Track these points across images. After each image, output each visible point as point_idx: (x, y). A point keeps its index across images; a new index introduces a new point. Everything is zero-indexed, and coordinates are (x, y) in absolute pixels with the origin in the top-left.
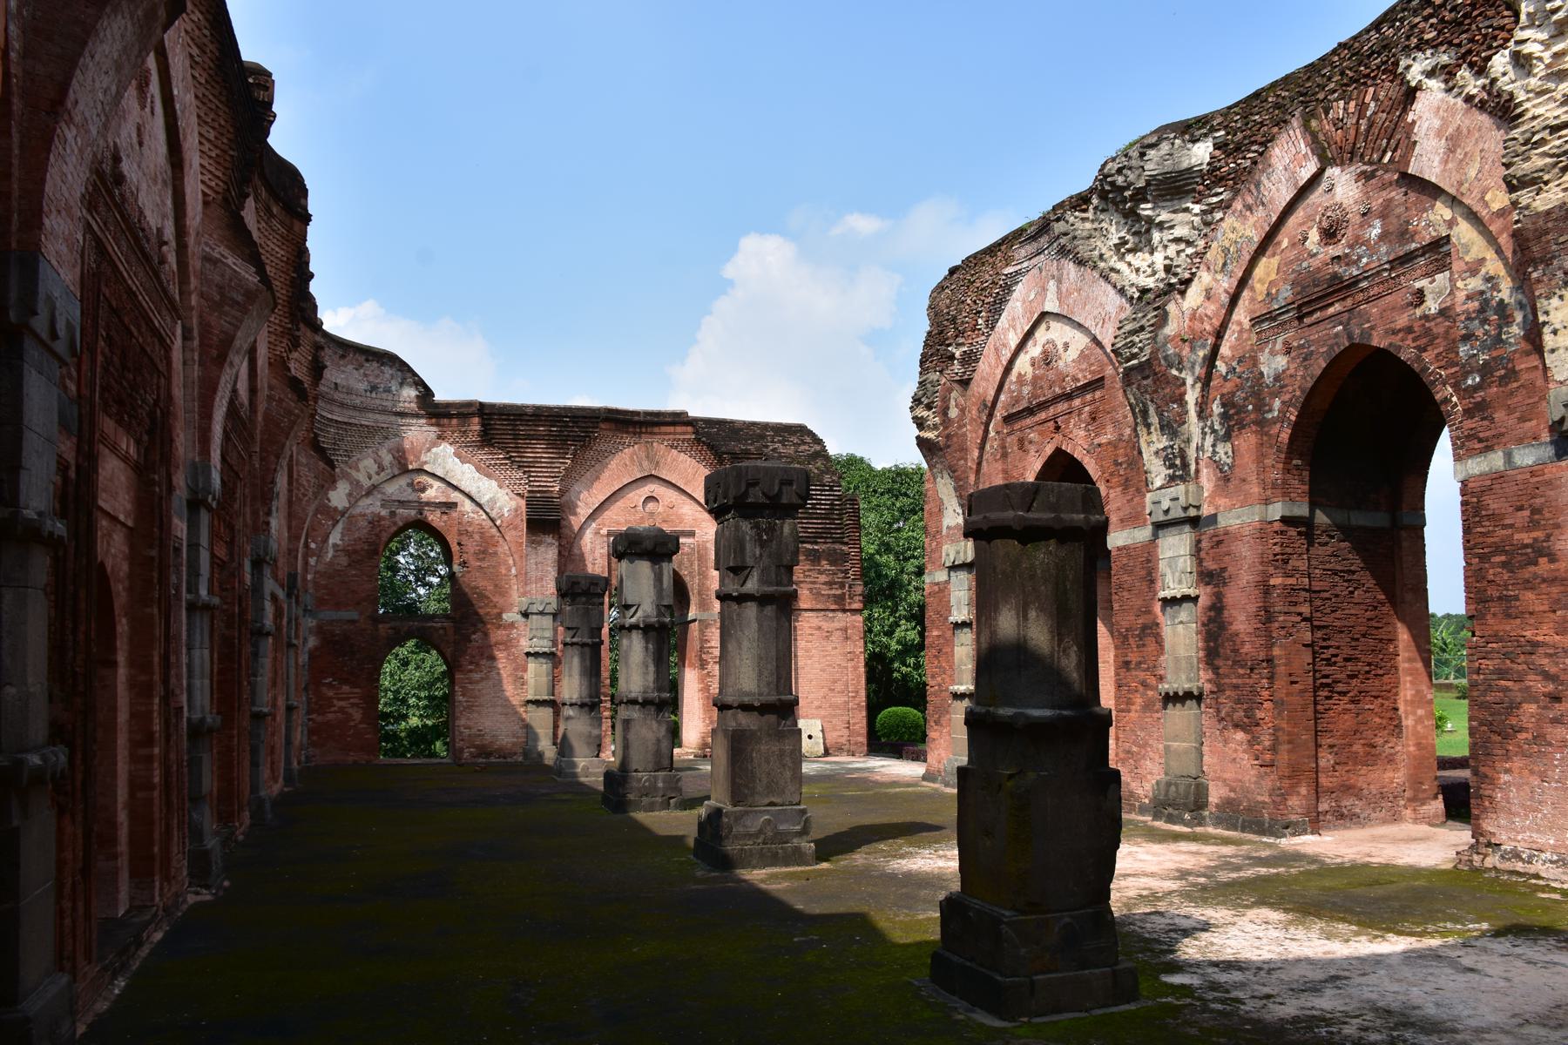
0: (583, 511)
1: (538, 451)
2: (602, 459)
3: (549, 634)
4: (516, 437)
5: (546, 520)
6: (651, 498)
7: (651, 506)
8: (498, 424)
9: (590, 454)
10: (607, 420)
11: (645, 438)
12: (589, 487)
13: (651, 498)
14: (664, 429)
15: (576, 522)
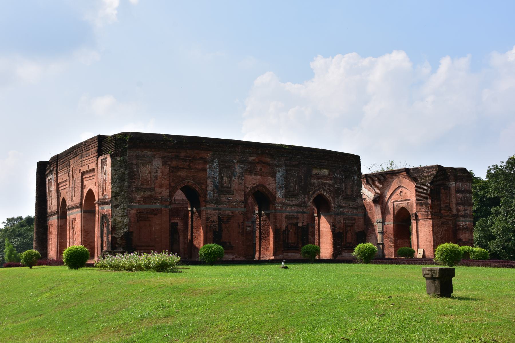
0: (388, 197)
1: (376, 184)
2: (390, 184)
3: (381, 227)
4: (372, 181)
5: (379, 200)
6: (401, 192)
7: (402, 194)
8: (369, 179)
9: (386, 183)
10: (388, 174)
11: (398, 176)
12: (388, 191)
13: (401, 192)
14: (402, 173)
15: (386, 199)
